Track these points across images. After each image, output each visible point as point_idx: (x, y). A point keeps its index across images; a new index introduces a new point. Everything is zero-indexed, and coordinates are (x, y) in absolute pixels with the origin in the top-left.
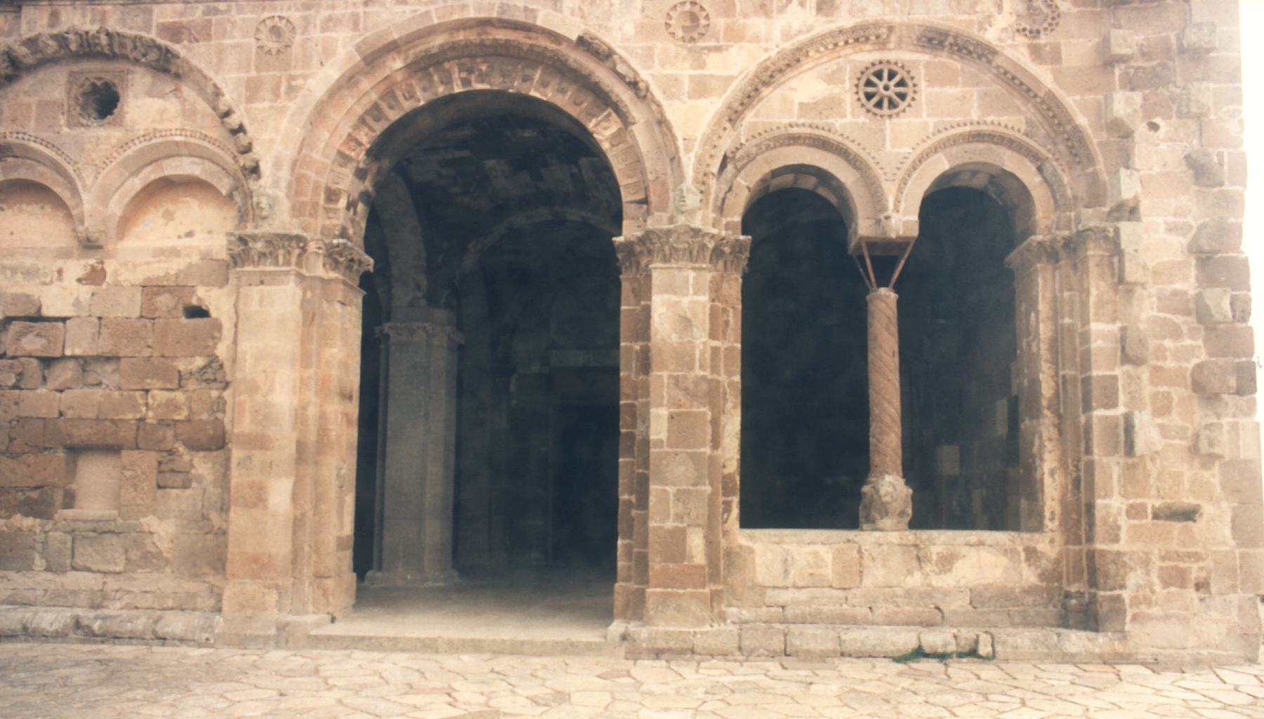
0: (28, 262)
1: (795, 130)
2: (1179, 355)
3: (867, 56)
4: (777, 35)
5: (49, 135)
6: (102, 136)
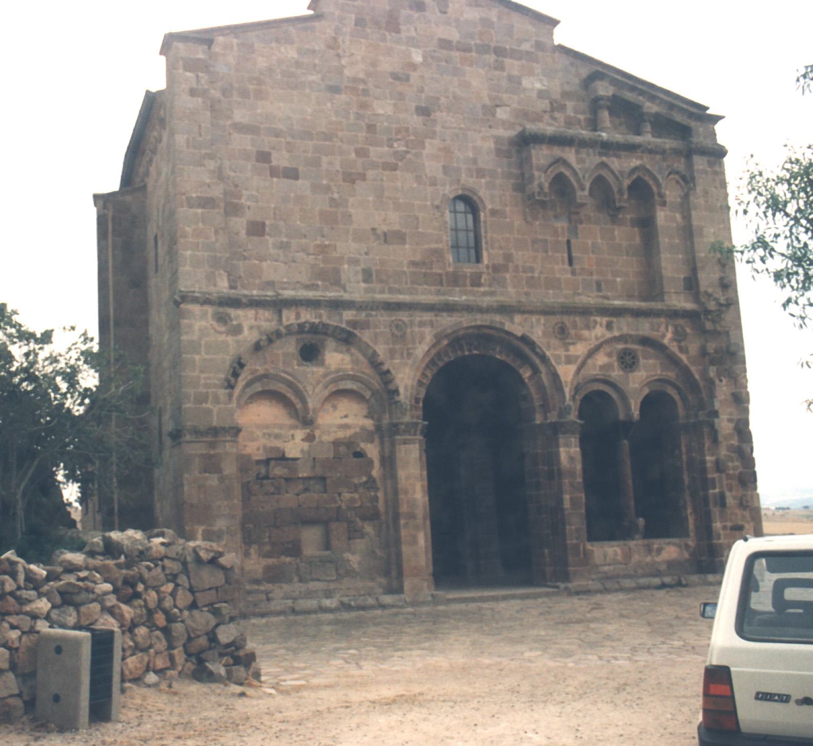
0: (276, 431)
1: (598, 377)
2: (735, 468)
3: (620, 346)
4: (593, 338)
5: (289, 370)
6: (314, 371)
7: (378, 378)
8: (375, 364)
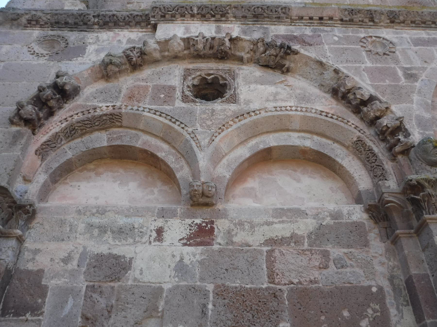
0: (122, 221)
7: (354, 119)
8: (342, 93)
